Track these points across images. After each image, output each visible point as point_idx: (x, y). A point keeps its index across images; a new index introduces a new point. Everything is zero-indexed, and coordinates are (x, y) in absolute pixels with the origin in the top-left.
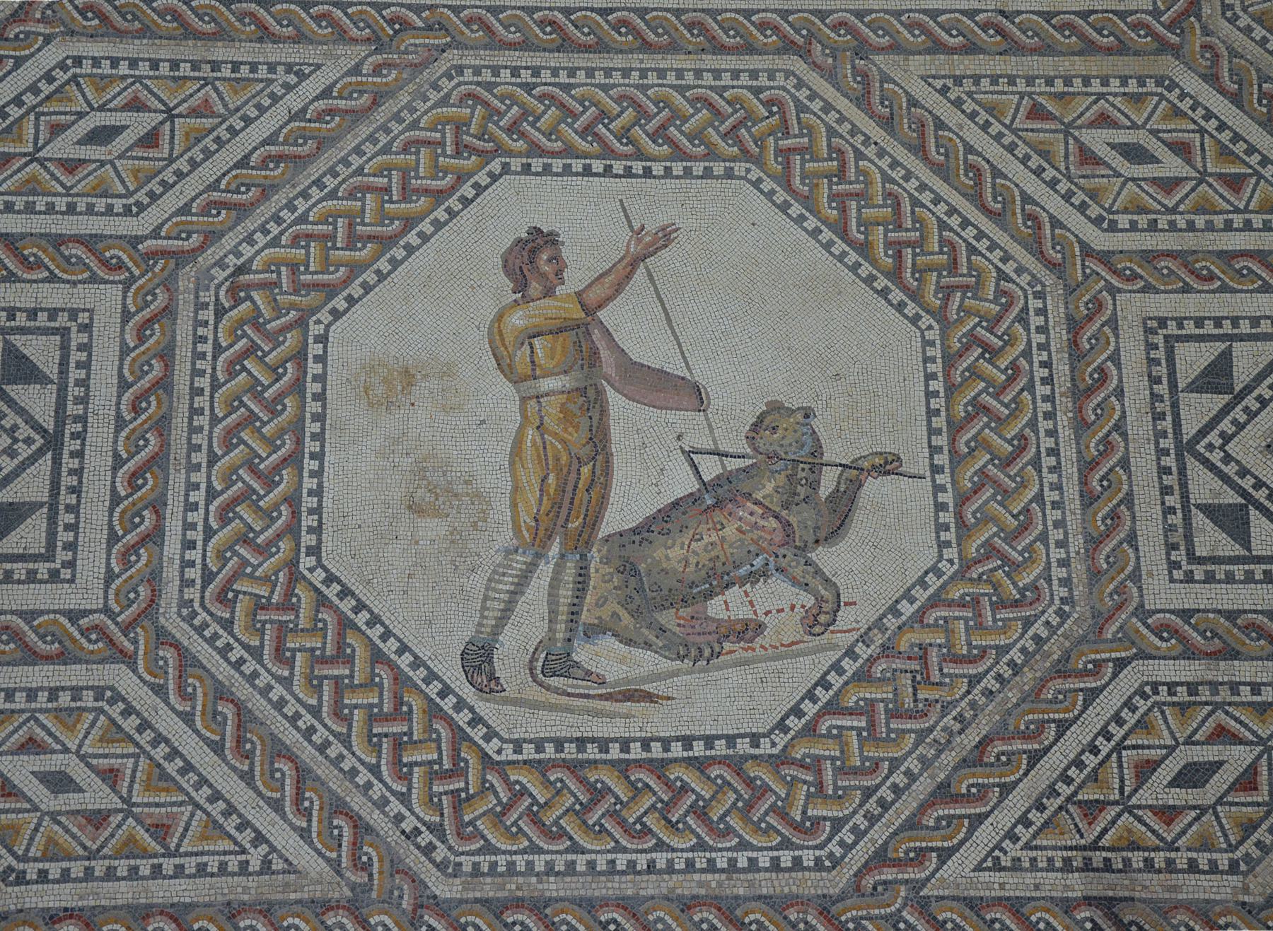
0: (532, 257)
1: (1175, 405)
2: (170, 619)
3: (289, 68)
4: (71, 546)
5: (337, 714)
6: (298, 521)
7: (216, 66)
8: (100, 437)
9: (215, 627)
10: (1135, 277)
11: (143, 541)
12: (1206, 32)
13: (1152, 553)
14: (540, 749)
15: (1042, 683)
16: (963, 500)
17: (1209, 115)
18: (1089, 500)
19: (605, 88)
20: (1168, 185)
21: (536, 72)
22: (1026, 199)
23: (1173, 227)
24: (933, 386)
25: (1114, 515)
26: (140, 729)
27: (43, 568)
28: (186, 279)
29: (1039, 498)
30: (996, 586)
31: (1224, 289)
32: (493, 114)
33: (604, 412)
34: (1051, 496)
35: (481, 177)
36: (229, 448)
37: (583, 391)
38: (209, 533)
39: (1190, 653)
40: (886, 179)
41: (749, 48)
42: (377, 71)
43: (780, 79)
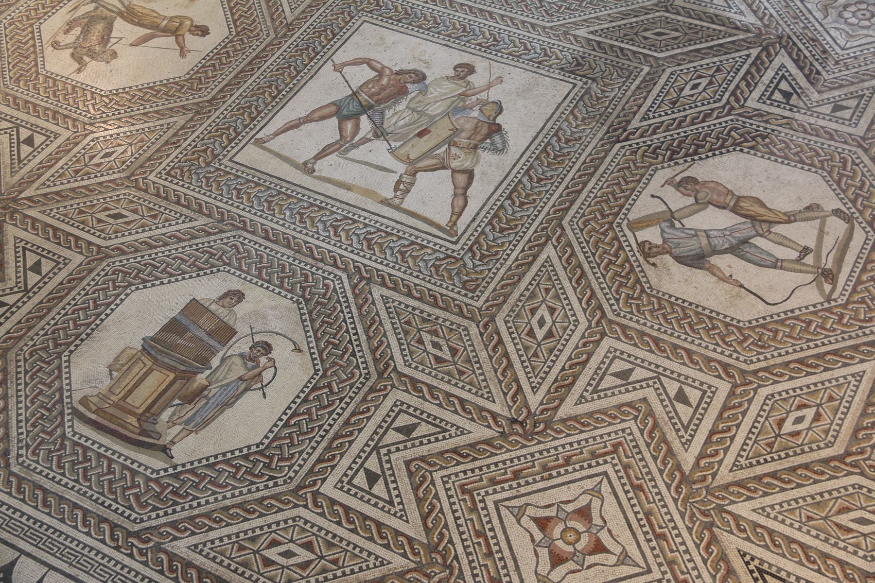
0: (204, 31)
20: (91, 158)
25: (18, 105)
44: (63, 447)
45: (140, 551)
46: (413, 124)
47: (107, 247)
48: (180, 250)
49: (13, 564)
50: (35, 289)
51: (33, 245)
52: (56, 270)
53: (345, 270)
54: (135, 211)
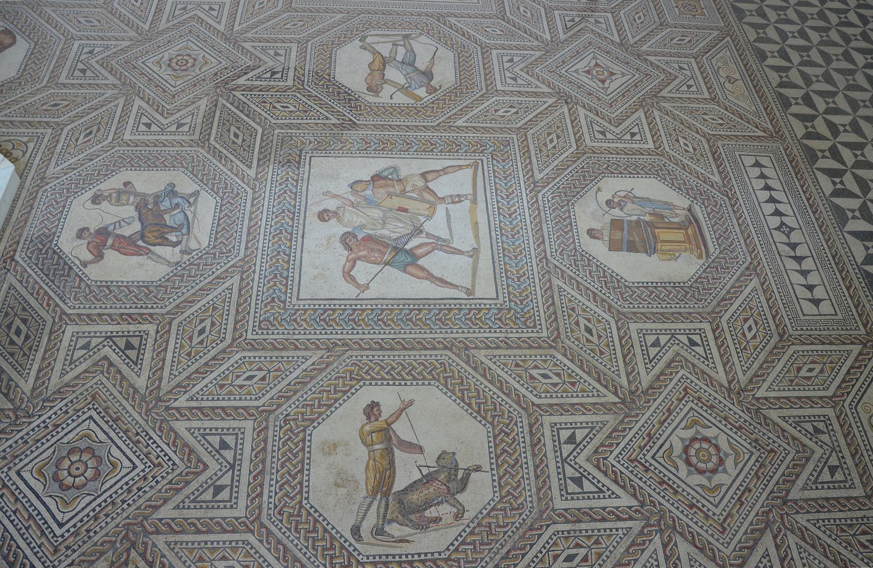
1: (560, 448)
2: (264, 519)
3: (303, 357)
4: (237, 498)
5: (313, 548)
6: (302, 489)
7: (282, 358)
8: (246, 465)
9: (277, 522)
10: (547, 411)
11: (257, 496)
12: (562, 343)
13: (556, 492)
14: (374, 558)
15: (525, 532)
16: (500, 478)
17: (565, 365)
18: (537, 477)
19: (393, 360)
20: (555, 385)
21: (373, 356)
22: (515, 389)
23: (557, 396)
24: (491, 444)
25: (544, 481)
26: (255, 553)
27: (228, 504)
28: (271, 418)
29: (523, 477)
30: (511, 504)
31: (572, 414)
32: (361, 368)
33: (393, 455)
34: (526, 476)
35: (357, 387)
36: (282, 468)
37: (387, 449)
38: (276, 493)
39: (567, 522)
40: (475, 384)
41: (435, 349)
42: (328, 357)
43: (444, 357)
44: (725, 249)
45: (731, 190)
46: (398, 219)
47: (613, 317)
48: (585, 278)
49: (775, 229)
50: (668, 332)
51: (644, 359)
52: (649, 332)
53: (536, 196)
54: (577, 324)
